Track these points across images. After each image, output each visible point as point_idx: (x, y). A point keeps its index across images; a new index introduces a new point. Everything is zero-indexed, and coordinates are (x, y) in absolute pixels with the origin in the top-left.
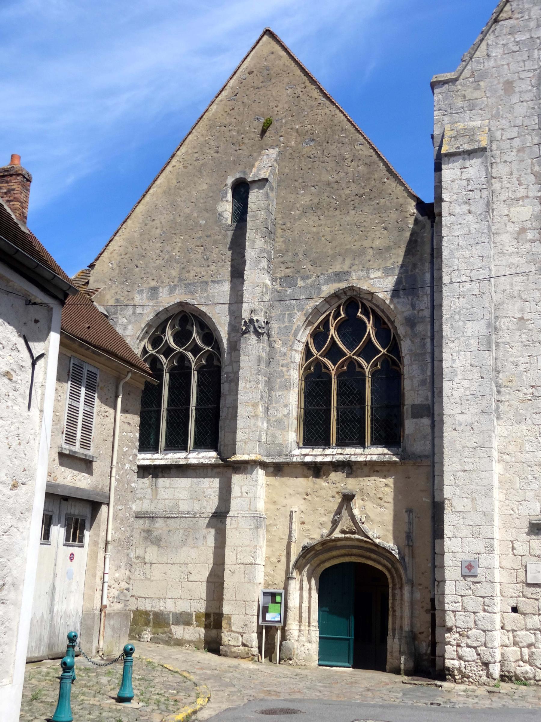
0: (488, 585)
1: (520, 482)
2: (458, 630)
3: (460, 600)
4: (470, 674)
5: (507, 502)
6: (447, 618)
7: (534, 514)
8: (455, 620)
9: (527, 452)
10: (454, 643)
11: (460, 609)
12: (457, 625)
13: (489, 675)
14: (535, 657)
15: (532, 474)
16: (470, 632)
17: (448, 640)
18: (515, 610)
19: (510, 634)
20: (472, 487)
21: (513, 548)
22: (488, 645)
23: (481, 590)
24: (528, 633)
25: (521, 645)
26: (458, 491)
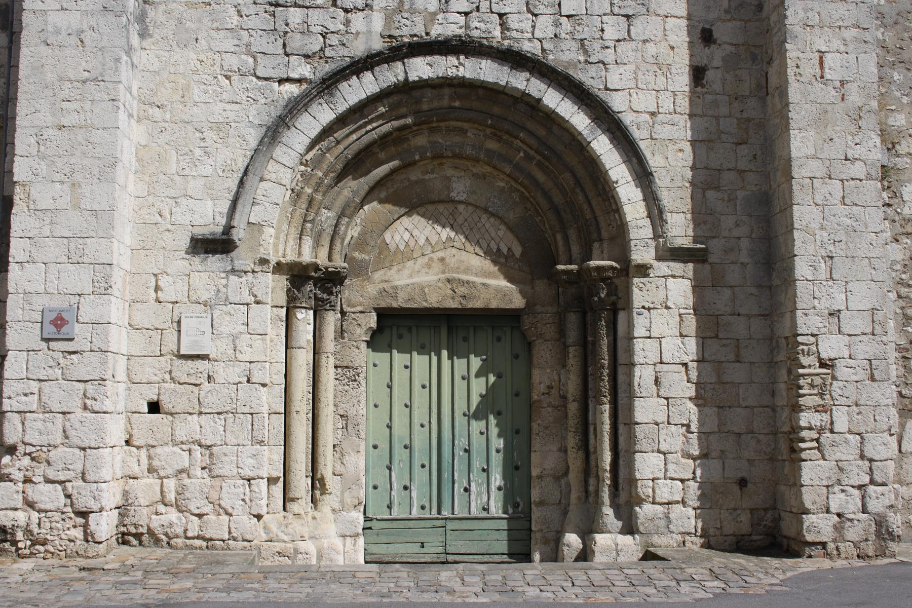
0: (95, 358)
1: (178, 161)
2: (29, 449)
3: (36, 391)
4: (48, 537)
5: (151, 199)
6: (7, 427)
7: (202, 222)
8: (23, 431)
9: (196, 104)
10: (18, 476)
11: (34, 408)
12: (26, 440)
13: (88, 536)
14: (187, 495)
15: (202, 145)
16: (51, 454)
17: (6, 471)
18: (154, 407)
19: (144, 451)
20: (73, 161)
21: (157, 289)
22: (88, 477)
23: (82, 367)
24: (177, 449)
25: (162, 473)
26: (43, 168)
